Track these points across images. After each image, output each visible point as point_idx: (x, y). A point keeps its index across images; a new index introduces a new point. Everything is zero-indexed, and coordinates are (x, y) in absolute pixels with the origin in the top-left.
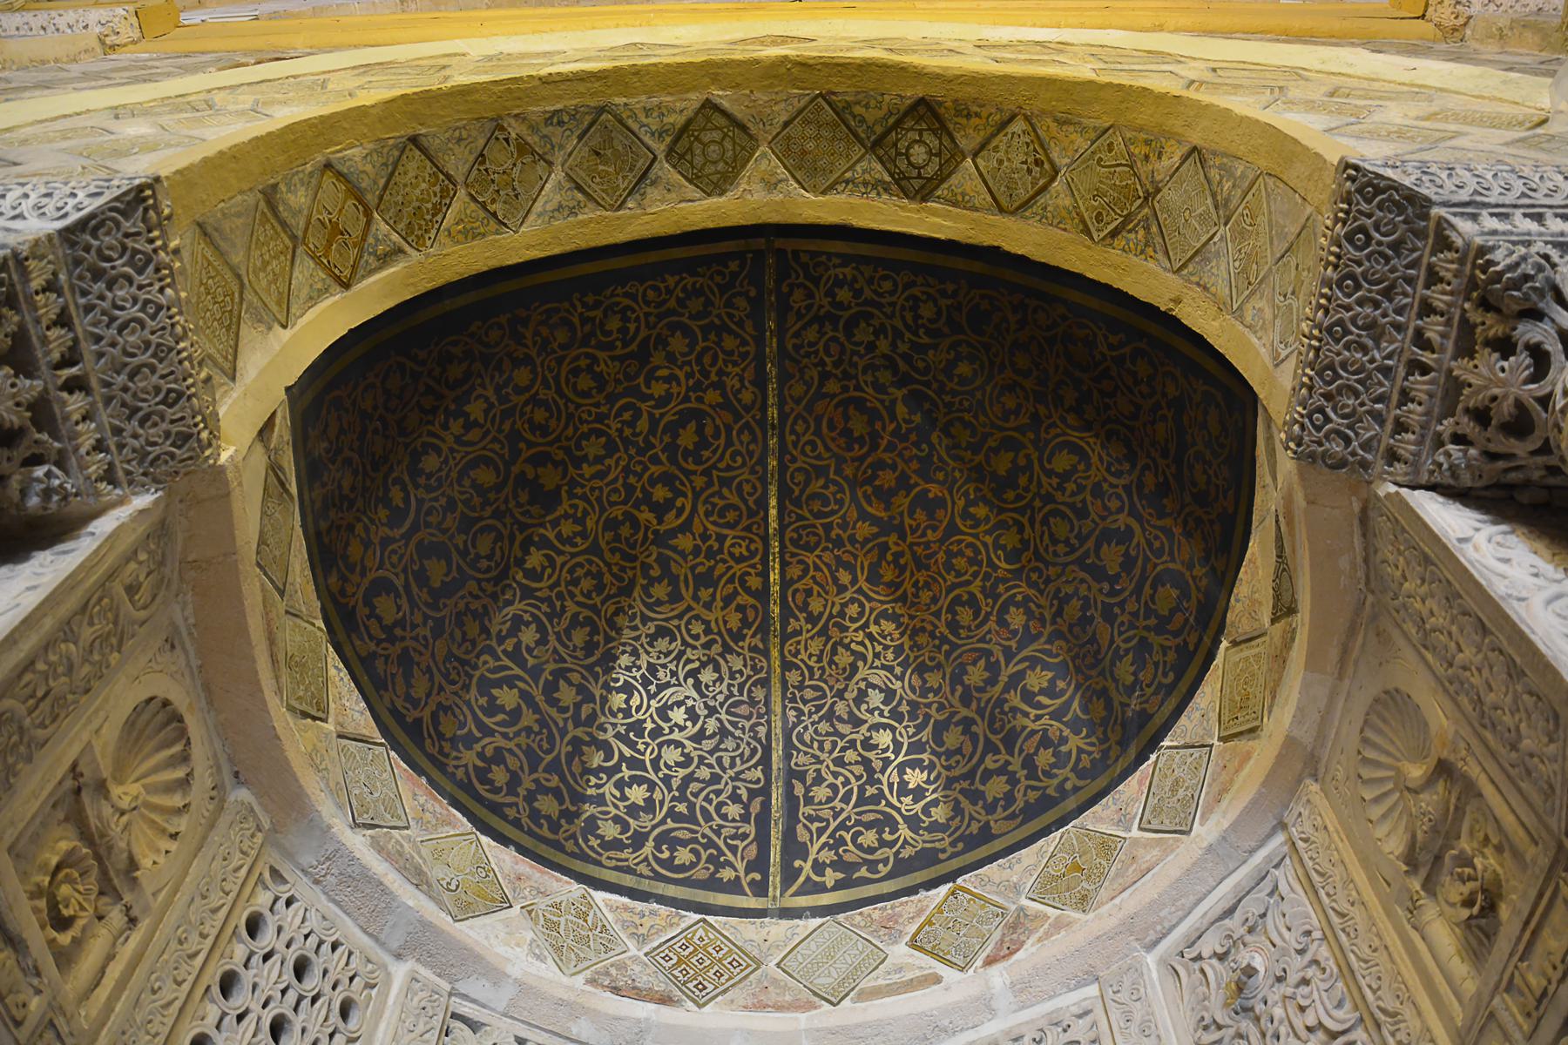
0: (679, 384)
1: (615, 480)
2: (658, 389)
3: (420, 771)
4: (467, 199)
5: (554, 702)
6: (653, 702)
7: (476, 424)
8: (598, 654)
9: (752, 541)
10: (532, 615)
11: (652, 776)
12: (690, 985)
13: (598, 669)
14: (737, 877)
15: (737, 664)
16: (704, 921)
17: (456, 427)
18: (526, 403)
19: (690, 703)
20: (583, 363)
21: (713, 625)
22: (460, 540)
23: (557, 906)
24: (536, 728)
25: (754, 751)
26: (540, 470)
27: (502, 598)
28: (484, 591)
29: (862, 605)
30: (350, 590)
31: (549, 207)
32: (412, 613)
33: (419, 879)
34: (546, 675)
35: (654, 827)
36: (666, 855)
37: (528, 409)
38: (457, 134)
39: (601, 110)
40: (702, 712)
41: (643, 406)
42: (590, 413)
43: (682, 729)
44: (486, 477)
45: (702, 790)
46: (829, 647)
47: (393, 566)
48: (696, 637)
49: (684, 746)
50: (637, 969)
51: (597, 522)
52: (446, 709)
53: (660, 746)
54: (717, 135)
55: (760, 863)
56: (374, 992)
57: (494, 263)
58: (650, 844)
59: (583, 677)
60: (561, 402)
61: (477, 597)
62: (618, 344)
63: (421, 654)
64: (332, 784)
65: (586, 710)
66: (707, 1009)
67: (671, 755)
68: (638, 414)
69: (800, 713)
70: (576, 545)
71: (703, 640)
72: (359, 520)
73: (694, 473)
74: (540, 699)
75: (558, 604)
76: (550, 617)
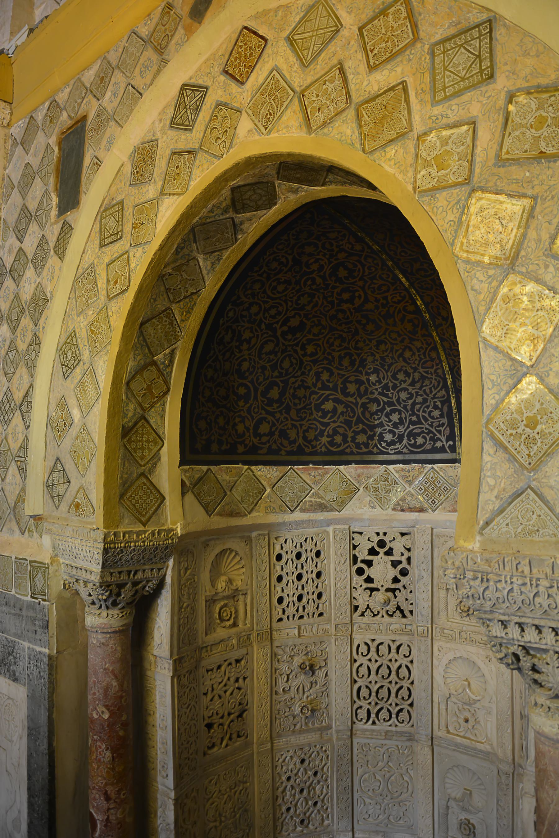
0: (322, 260)
1: (323, 303)
2: (315, 267)
3: (307, 463)
4: (178, 305)
5: (347, 395)
6: (389, 374)
7: (251, 338)
8: (357, 363)
9: (400, 293)
10: (322, 368)
11: (399, 408)
12: (430, 501)
13: (360, 369)
14: (443, 445)
15: (418, 344)
16: (433, 468)
17: (245, 346)
18: (264, 314)
19: (404, 369)
20: (274, 284)
21: (401, 332)
22: (276, 373)
23: (376, 480)
24: (345, 410)
25: (439, 382)
27: (306, 371)
28: (298, 377)
30: (247, 442)
32: (274, 417)
33: (321, 507)
34: (340, 386)
35: (405, 430)
36: (413, 442)
37: (266, 315)
38: (152, 300)
39: (193, 229)
40: (411, 371)
41: (314, 275)
42: (293, 293)
43: (405, 382)
44: (269, 347)
45: (421, 408)
48: (396, 339)
49: (408, 390)
50: (409, 498)
51: (326, 320)
52: (307, 431)
53: (398, 392)
56: (325, 541)
58: (406, 438)
59: (356, 376)
60: (278, 301)
61: (296, 381)
62: (283, 268)
63: (286, 425)
65: (362, 389)
67: (403, 395)
68: (313, 280)
70: (323, 333)
71: (399, 339)
72: (234, 419)
73: (356, 282)
74: (341, 397)
75: (330, 357)
76: (329, 364)
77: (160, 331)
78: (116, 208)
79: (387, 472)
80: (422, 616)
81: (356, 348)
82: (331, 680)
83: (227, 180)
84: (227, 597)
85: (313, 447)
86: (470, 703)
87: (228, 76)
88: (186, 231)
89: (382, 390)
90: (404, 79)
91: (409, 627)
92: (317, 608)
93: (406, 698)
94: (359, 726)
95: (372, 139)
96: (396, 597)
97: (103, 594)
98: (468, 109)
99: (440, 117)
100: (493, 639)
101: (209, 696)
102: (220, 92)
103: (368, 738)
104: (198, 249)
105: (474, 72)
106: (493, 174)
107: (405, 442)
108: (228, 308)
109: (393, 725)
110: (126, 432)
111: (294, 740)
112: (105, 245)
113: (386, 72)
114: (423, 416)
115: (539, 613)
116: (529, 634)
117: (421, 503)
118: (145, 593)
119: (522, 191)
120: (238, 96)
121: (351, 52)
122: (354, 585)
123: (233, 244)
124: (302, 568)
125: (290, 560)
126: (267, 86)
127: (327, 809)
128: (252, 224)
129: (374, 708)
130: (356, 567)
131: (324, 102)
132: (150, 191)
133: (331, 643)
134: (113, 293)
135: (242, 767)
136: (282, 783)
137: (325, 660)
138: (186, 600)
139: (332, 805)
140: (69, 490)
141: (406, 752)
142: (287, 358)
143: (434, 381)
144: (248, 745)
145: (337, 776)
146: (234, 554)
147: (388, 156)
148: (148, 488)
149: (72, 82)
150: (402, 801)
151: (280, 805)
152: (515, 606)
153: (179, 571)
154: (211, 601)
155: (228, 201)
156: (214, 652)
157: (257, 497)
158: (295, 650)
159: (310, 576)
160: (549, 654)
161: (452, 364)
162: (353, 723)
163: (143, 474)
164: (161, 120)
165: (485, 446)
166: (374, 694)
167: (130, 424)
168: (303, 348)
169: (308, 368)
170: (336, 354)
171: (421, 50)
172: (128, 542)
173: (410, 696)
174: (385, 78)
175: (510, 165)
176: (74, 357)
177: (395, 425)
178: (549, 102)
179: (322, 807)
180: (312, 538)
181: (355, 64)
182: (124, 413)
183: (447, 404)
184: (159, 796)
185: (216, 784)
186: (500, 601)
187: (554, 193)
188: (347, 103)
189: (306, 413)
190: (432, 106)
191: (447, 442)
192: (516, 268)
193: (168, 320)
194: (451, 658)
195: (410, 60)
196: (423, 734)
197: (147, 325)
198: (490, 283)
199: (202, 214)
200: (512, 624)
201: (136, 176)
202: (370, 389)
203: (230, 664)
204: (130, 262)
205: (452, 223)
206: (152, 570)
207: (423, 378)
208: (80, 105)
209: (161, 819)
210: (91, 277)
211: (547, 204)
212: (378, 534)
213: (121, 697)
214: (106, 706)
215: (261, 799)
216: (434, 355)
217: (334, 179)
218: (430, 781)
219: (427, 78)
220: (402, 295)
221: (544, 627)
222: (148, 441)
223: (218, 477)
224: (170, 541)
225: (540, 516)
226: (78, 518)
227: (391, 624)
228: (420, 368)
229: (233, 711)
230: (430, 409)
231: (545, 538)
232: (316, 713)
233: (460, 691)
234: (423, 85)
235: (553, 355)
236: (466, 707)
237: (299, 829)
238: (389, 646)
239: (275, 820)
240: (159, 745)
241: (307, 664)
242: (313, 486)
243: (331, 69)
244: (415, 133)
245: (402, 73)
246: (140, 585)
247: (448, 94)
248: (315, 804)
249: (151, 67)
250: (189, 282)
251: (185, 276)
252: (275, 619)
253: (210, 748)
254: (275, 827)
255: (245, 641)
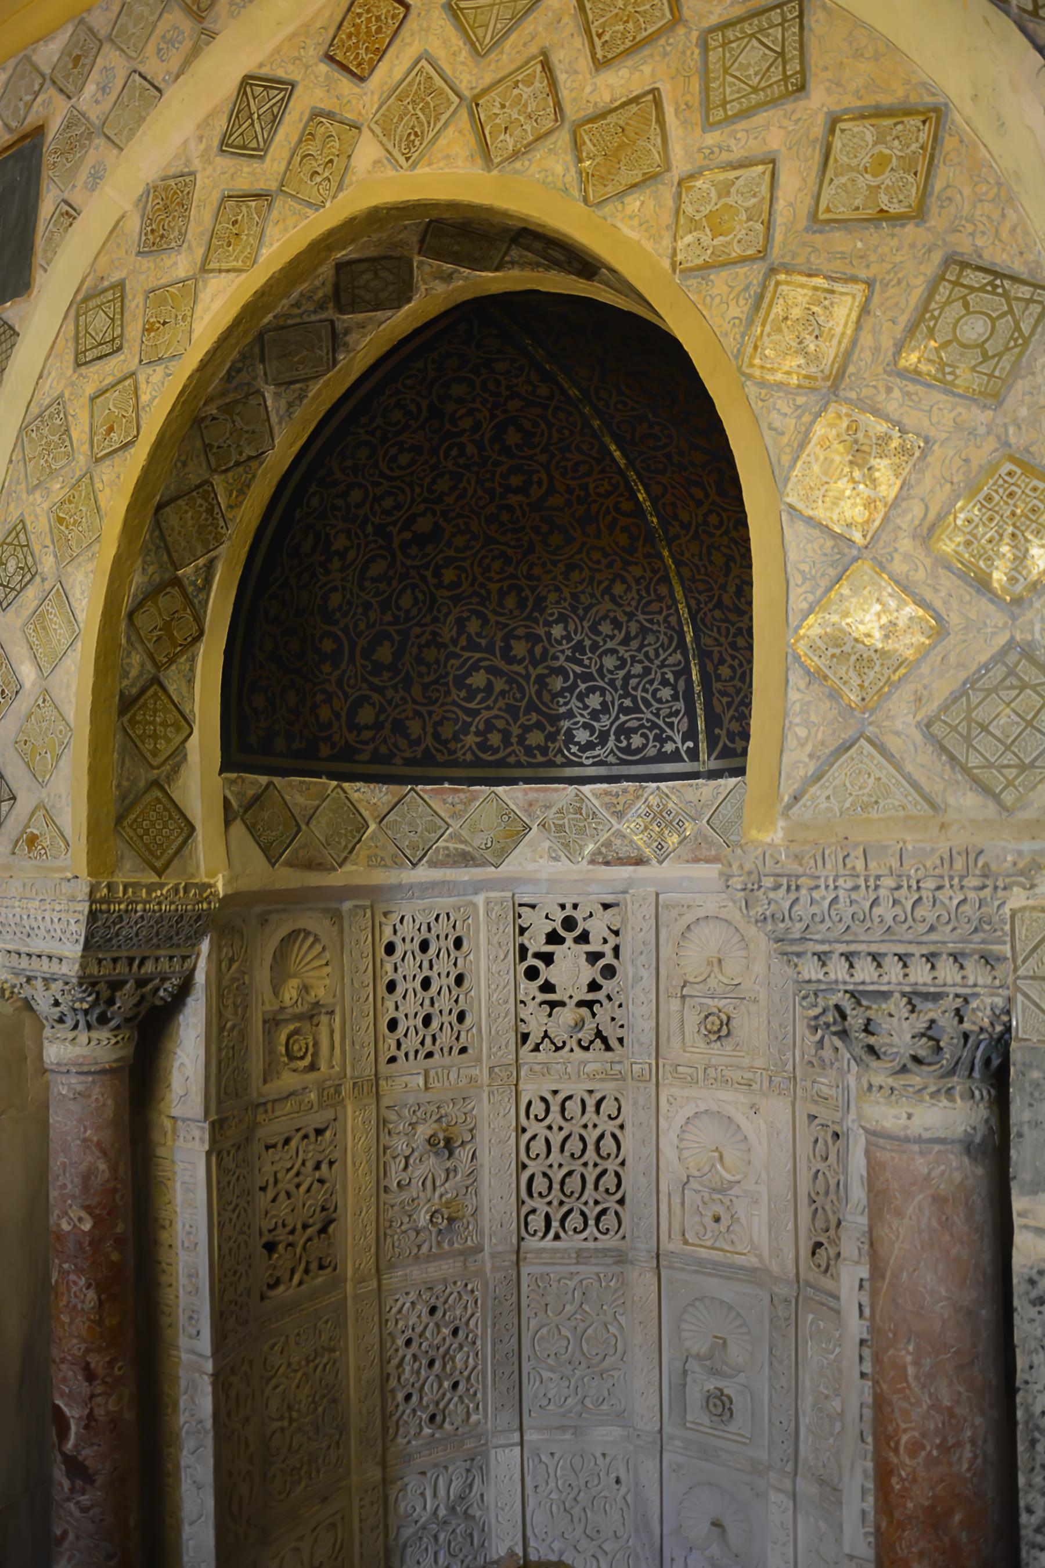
1: (475, 492)
2: (466, 423)
3: (439, 781)
5: (511, 660)
6: (586, 624)
7: (347, 549)
8: (530, 604)
9: (610, 478)
10: (469, 610)
11: (601, 683)
13: (536, 614)
15: (638, 571)
16: (658, 788)
17: (336, 564)
19: (612, 615)
20: (394, 451)
21: (608, 549)
22: (388, 617)
23: (560, 811)
24: (507, 688)
26: (413, 528)
28: (425, 625)
29: (719, 515)
30: (336, 738)
31: (281, 412)
32: (384, 696)
33: (466, 859)
34: (499, 644)
35: (612, 724)
36: (624, 744)
37: (376, 507)
38: (179, 465)
39: (260, 336)
40: (623, 619)
42: (424, 470)
43: (612, 638)
44: (377, 568)
45: (639, 683)
46: (704, 549)
47: (352, 687)
48: (598, 562)
49: (617, 652)
50: (618, 842)
53: (600, 657)
54: (368, 276)
55: (691, 734)
57: (275, 482)
58: (612, 737)
59: (527, 627)
60: (398, 483)
61: (423, 633)
63: (404, 711)
64: (389, 862)
65: (538, 650)
66: (665, 864)
67: (609, 662)
69: (699, 602)
73: (535, 455)
74: (502, 665)
75: (483, 592)
77: (190, 523)
78: (109, 295)
79: (581, 798)
80: (641, 1045)
81: (530, 577)
82: (482, 1166)
83: (330, 249)
84: (299, 1017)
85: (451, 752)
86: (722, 1189)
87: (334, 66)
88: (249, 338)
89: (573, 653)
90: (657, 85)
91: (617, 1067)
92: (457, 1039)
93: (613, 1189)
94: (532, 1243)
95: (596, 188)
96: (594, 1015)
97: (82, 1000)
98: (764, 139)
99: (716, 150)
100: (805, 985)
101: (270, 1193)
102: (319, 93)
103: (546, 1264)
104: (265, 374)
105: (774, 80)
106: (805, 244)
107: (611, 743)
108: (311, 490)
109: (591, 1239)
110: (127, 704)
111: (416, 1273)
112: (86, 363)
113: (624, 72)
114: (643, 698)
115: (878, 933)
116: (863, 970)
117: (638, 848)
118: (158, 1003)
119: (850, 271)
120: (354, 102)
121: (564, 35)
122: (521, 997)
123: (328, 371)
124: (431, 967)
125: (409, 954)
126: (410, 84)
127: (475, 1394)
128: (365, 335)
129: (558, 1211)
130: (525, 965)
131: (515, 116)
132: (180, 264)
133: (480, 1101)
134: (104, 448)
135: (327, 1322)
136: (397, 1350)
137: (471, 1130)
138: (230, 1017)
139: (485, 1387)
140: (14, 812)
141: (612, 1284)
142: (409, 591)
143: (662, 637)
144: (338, 1282)
145: (493, 1333)
146: (311, 939)
147: (629, 210)
148: (166, 809)
149: (11, 63)
150: (606, 1371)
151: (393, 1391)
152: (841, 925)
153: (220, 962)
154: (272, 1023)
155: (328, 289)
156: (278, 1113)
157: (354, 837)
158: (419, 1114)
159: (444, 981)
160: (893, 1000)
161: (694, 606)
162: (521, 1239)
163: (156, 783)
164: (201, 138)
165: (792, 678)
166: (556, 1186)
167: (134, 691)
168: (437, 573)
169: (444, 610)
170: (494, 587)
171: (686, 38)
172: (131, 903)
173: (619, 1186)
174: (622, 82)
175: (832, 230)
176: (22, 568)
177: (595, 715)
178: (894, 133)
179: (468, 1390)
180: (448, 914)
181: (571, 55)
182: (124, 670)
183: (683, 678)
184: (182, 1373)
185: (282, 1352)
186: (818, 919)
187: (900, 275)
188: (556, 121)
189: (438, 691)
190: (704, 131)
191: (683, 744)
192: (841, 393)
193: (205, 504)
194: (691, 1114)
195: (666, 54)
196: (643, 1249)
197: (168, 509)
198: (799, 417)
199: (279, 309)
200: (835, 956)
201: (150, 237)
202: (552, 651)
203: (306, 1137)
204: (140, 393)
205: (737, 321)
206: (171, 958)
207: (644, 631)
208: (29, 106)
209: (187, 1414)
210: (58, 422)
211: (891, 292)
212: (563, 907)
213: (115, 1191)
214: (87, 1208)
215: (360, 1380)
216: (663, 590)
217: (521, 256)
218: (656, 1330)
219: (696, 85)
220: (614, 481)
221: (885, 954)
222: (164, 724)
223: (287, 798)
224: (205, 906)
225: (879, 779)
226: (34, 862)
227: (585, 1063)
228: (639, 613)
229: (311, 1221)
230: (655, 686)
231: (888, 814)
232: (457, 1225)
233: (707, 1168)
234: (688, 98)
235: (900, 528)
236: (716, 1196)
237: (427, 1431)
238: (583, 1101)
239: (385, 1417)
240: (182, 1280)
241: (441, 1136)
242: (449, 821)
243: (527, 63)
244: (675, 175)
245: (653, 75)
246: (150, 986)
247: (730, 113)
248: (455, 1386)
249: (180, 43)
250: (246, 436)
251: (239, 424)
252: (383, 1059)
253: (271, 1287)
254: (385, 1429)
255: (331, 1096)
